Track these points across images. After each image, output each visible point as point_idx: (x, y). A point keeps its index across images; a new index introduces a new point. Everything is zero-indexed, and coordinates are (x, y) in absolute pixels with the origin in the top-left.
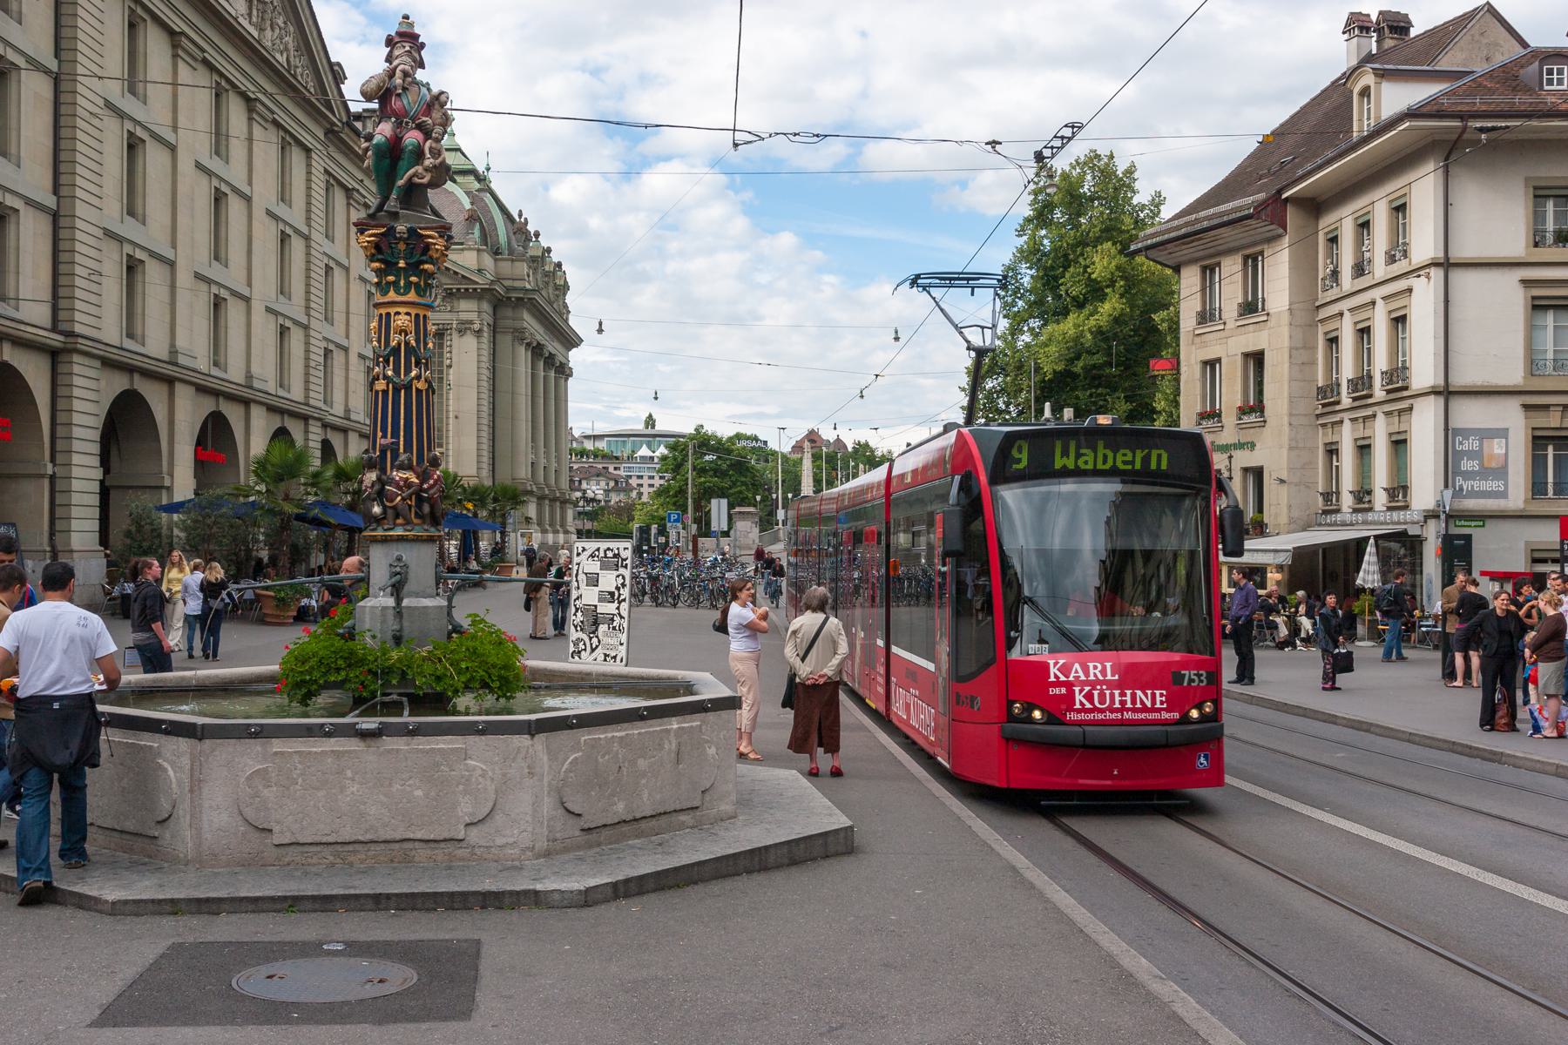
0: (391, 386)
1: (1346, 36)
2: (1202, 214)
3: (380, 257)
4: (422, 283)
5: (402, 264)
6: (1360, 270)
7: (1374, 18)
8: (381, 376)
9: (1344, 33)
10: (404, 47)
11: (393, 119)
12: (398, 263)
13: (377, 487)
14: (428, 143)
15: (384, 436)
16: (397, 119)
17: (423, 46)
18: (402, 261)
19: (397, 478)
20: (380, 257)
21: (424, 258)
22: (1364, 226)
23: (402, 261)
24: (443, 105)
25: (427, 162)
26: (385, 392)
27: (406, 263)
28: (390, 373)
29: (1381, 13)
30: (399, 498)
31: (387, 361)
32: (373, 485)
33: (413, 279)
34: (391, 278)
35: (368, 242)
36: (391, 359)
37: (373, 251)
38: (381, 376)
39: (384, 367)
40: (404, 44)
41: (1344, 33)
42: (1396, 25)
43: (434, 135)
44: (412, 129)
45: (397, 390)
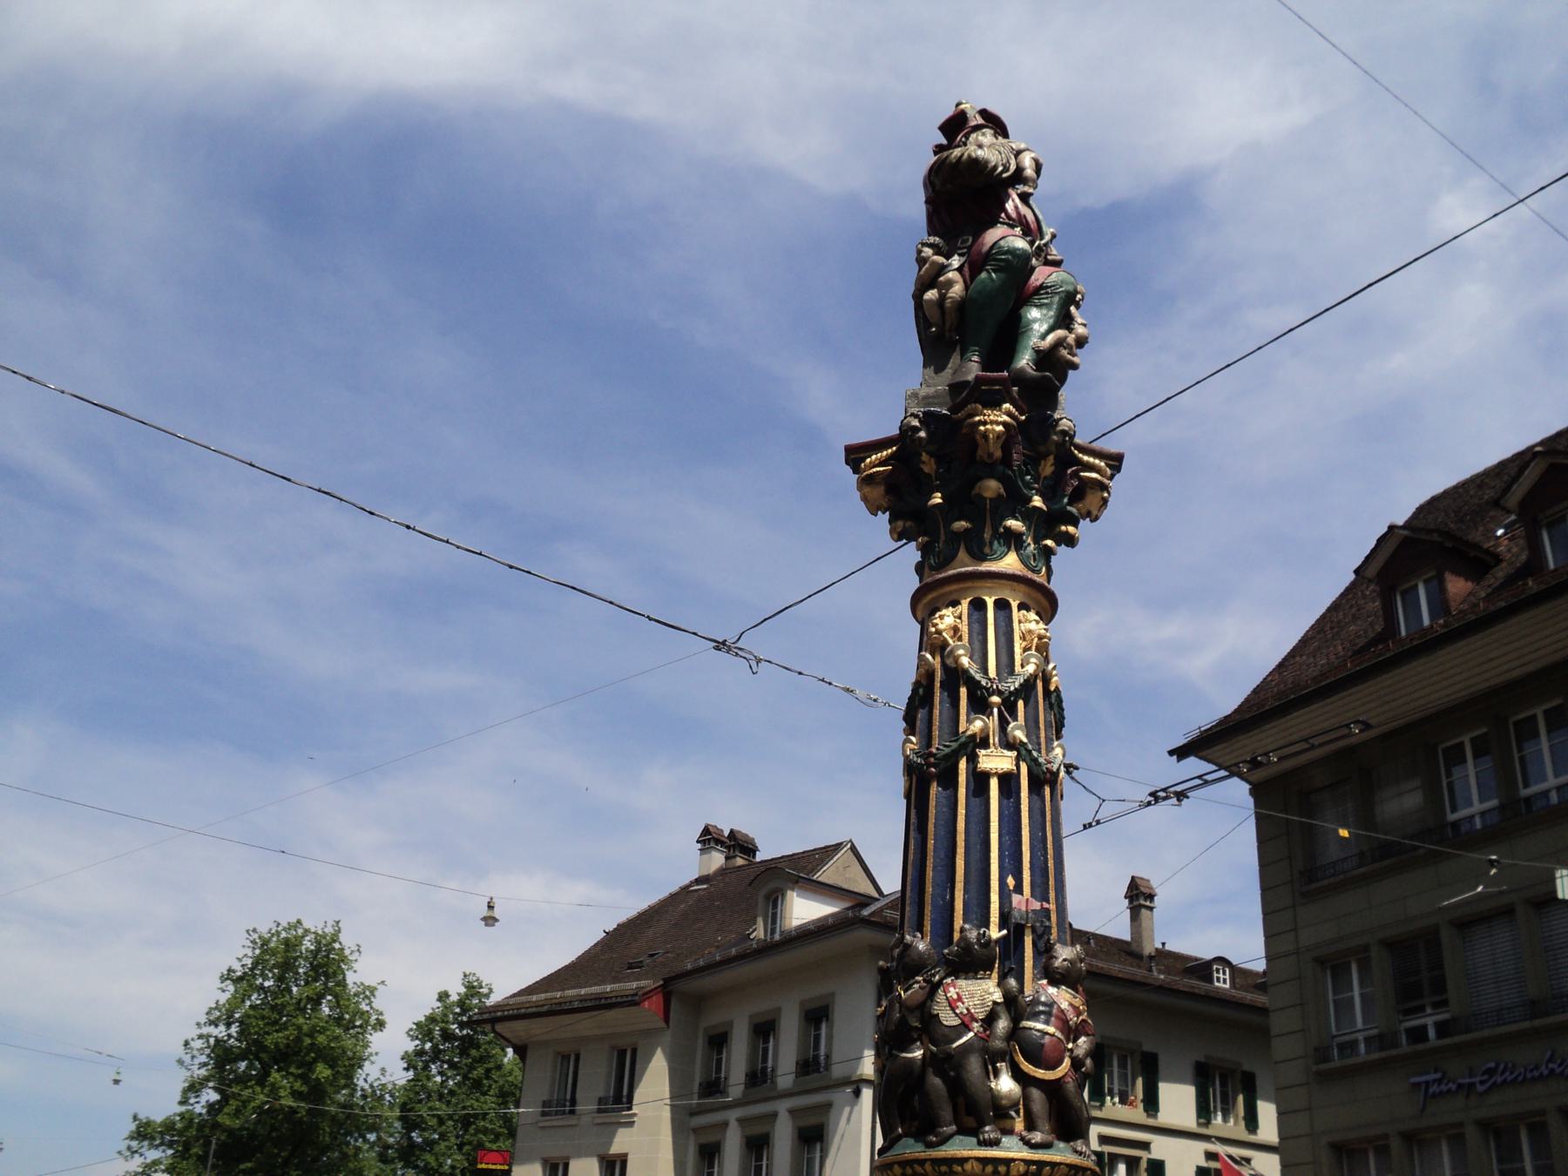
0: (1024, 768)
1: (699, 846)
2: (534, 998)
6: (758, 1078)
7: (726, 833)
8: (994, 739)
9: (698, 842)
12: (1030, 500)
13: (1002, 1025)
15: (1019, 889)
19: (1065, 1005)
22: (764, 1030)
26: (1008, 782)
28: (1020, 735)
29: (732, 831)
30: (1067, 1062)
31: (1009, 706)
32: (990, 1020)
36: (1021, 704)
38: (994, 739)
39: (1003, 724)
41: (698, 842)
42: (739, 845)
45: (1036, 784)
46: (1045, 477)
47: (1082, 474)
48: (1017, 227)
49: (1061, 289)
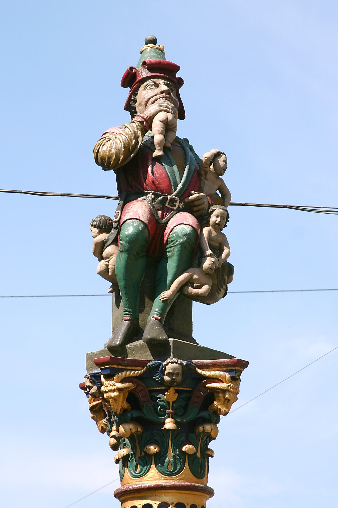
3: (135, 414)
4: (199, 455)
5: (169, 424)
10: (157, 86)
11: (150, 196)
12: (164, 423)
14: (205, 231)
16: (157, 196)
17: (180, 82)
18: (168, 420)
20: (135, 414)
21: (204, 414)
23: (168, 420)
24: (221, 171)
25: (207, 263)
27: (176, 423)
33: (186, 448)
34: (153, 449)
35: (119, 390)
37: (126, 405)
40: (157, 81)
43: (213, 219)
44: (179, 210)
46: (174, 402)
47: (207, 386)
48: (149, 193)
49: (178, 243)
